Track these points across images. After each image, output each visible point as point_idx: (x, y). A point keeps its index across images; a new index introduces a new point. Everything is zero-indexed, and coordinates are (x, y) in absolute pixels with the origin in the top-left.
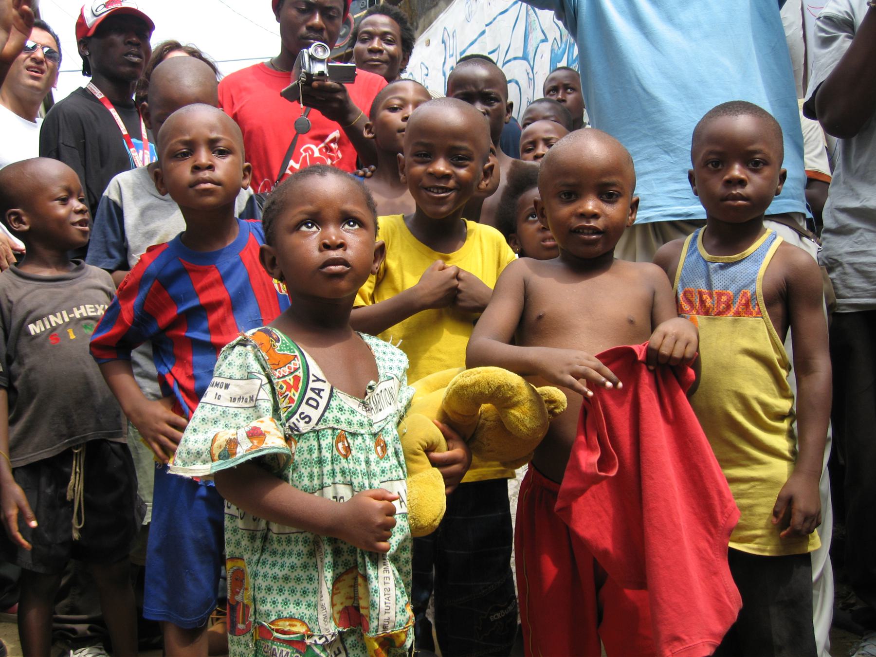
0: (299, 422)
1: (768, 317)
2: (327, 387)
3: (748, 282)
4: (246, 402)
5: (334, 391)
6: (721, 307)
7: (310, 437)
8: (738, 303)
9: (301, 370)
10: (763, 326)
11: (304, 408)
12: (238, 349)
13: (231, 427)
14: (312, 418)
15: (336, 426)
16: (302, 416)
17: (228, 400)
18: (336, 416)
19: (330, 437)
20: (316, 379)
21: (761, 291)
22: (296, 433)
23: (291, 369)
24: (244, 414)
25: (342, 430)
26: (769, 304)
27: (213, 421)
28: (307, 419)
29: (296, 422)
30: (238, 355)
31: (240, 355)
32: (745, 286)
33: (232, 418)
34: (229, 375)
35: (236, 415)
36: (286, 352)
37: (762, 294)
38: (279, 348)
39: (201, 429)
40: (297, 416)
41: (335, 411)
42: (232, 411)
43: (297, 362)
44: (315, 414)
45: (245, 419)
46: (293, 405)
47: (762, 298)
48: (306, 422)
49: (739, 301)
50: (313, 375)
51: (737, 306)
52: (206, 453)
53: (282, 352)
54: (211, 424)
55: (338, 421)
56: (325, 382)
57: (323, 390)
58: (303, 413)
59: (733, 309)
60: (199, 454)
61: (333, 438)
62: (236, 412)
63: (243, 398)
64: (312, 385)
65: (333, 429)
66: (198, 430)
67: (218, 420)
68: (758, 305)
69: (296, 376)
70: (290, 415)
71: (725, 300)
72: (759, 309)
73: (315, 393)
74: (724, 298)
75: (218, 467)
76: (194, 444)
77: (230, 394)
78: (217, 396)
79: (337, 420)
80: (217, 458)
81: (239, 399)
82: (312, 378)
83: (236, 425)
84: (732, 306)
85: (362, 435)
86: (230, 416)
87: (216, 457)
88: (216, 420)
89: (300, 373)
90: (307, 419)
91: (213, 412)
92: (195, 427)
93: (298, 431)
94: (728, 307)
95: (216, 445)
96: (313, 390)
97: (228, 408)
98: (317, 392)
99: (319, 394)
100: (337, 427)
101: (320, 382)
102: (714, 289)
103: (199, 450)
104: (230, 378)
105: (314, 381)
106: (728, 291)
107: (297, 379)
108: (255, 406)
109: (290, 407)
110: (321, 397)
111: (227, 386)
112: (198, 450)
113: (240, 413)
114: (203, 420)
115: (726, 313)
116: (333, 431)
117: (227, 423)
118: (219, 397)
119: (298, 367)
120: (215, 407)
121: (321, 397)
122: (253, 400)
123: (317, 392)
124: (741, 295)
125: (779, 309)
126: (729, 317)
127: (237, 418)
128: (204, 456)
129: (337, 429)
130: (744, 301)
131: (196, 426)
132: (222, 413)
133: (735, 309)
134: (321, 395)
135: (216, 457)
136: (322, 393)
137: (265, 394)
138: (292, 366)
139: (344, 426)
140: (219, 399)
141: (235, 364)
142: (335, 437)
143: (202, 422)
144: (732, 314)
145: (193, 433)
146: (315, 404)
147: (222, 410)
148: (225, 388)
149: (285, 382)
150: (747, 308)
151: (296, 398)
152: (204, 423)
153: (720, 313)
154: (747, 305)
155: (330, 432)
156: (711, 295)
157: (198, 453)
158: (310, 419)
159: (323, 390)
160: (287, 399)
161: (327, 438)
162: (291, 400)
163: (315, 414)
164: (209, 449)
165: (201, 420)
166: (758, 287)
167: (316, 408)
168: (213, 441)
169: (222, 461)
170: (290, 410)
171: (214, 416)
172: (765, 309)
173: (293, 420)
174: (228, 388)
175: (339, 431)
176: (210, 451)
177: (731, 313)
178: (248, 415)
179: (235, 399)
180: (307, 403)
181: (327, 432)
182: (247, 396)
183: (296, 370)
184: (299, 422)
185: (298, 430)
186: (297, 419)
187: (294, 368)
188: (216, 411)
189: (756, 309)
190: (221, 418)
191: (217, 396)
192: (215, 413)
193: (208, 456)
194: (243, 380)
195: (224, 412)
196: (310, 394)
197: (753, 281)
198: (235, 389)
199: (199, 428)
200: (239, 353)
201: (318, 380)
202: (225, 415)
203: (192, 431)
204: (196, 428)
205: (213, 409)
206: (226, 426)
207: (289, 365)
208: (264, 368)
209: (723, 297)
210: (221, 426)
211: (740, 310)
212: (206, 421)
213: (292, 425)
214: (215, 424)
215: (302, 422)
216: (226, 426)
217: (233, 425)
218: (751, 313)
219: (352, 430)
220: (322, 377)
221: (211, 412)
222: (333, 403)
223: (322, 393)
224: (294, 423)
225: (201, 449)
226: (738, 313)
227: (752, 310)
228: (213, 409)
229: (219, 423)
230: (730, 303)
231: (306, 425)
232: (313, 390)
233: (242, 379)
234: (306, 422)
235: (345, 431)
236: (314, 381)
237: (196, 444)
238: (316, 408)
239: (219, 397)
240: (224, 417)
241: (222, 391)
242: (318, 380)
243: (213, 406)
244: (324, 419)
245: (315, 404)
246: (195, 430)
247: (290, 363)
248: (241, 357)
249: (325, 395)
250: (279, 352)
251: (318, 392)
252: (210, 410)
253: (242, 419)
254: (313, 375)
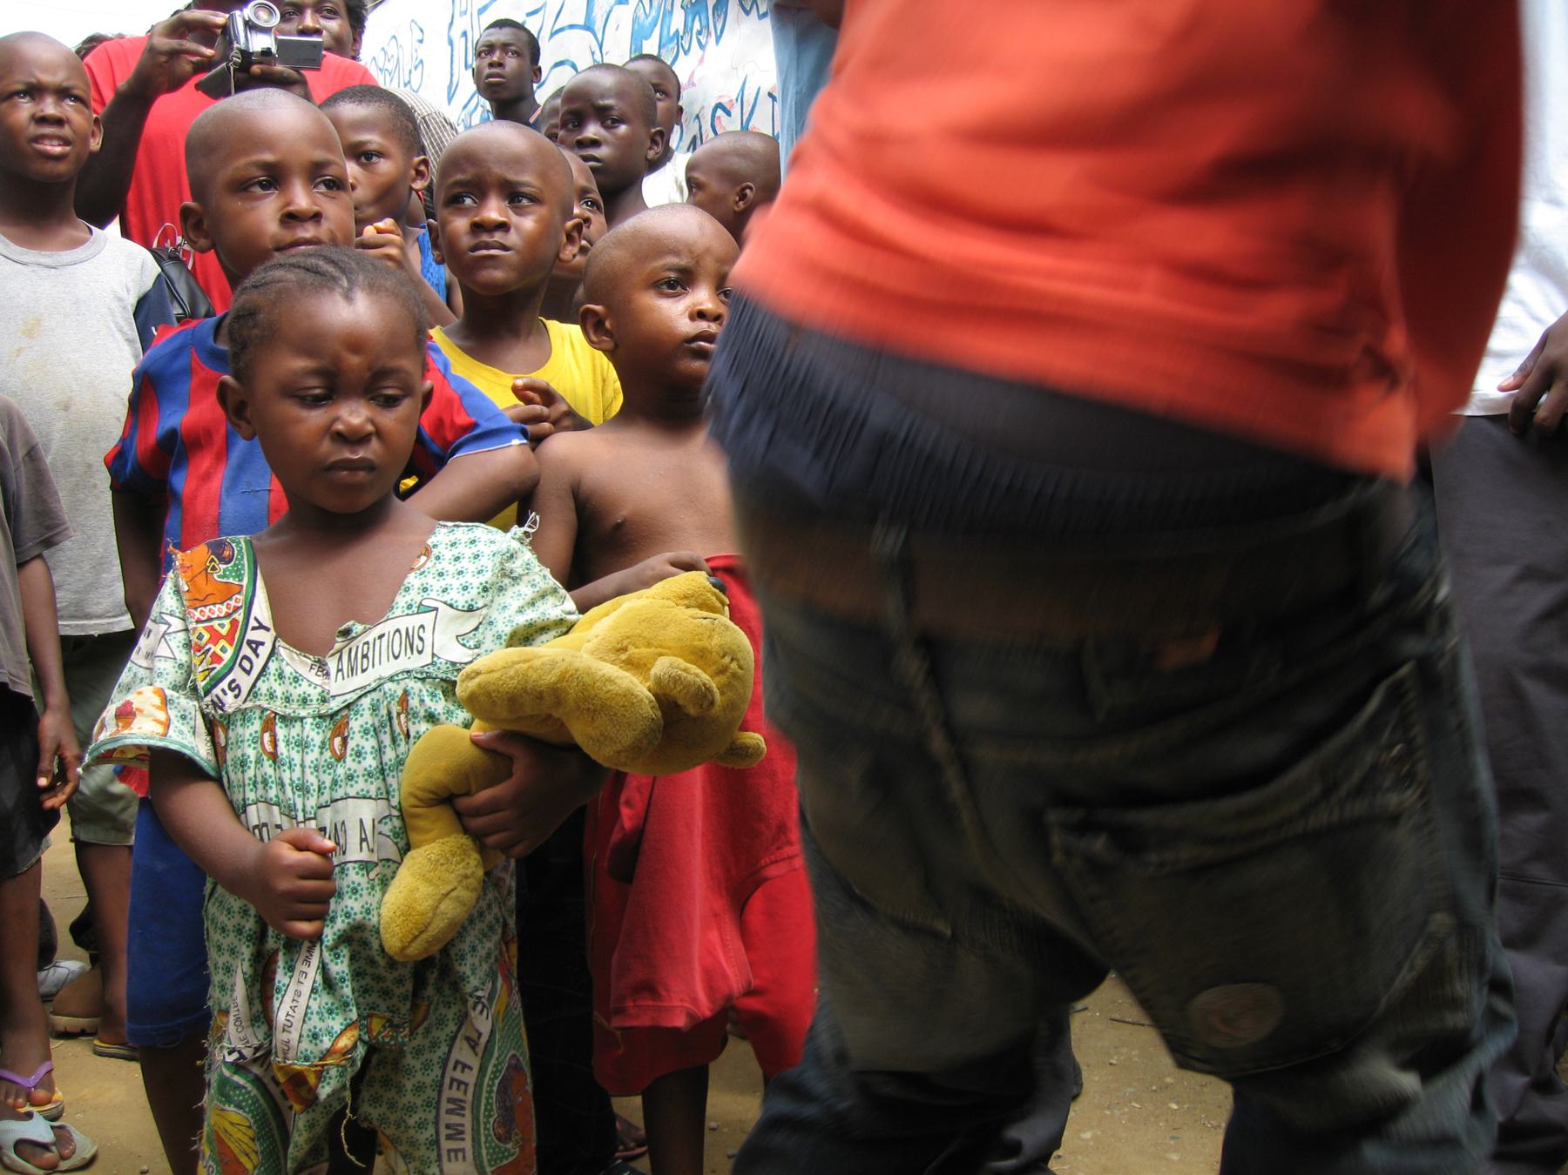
0: (225, 694)
5: (277, 644)
20: (257, 625)
22: (220, 712)
29: (221, 695)
36: (231, 580)
40: (224, 684)
44: (245, 682)
50: (256, 619)
53: (225, 580)
55: (272, 696)
57: (262, 644)
65: (264, 710)
70: (213, 683)
73: (251, 648)
79: (271, 694)
82: (253, 623)
85: (302, 719)
89: (240, 616)
93: (223, 710)
98: (254, 646)
99: (255, 651)
101: (262, 631)
105: (254, 629)
107: (234, 623)
109: (214, 668)
110: (257, 656)
119: (240, 605)
121: (257, 656)
123: (254, 646)
134: (259, 651)
138: (233, 603)
146: (246, 664)
149: (210, 629)
155: (258, 713)
159: (262, 644)
162: (217, 658)
163: (245, 682)
167: (248, 672)
170: (212, 674)
173: (217, 691)
175: (268, 712)
183: (236, 609)
184: (225, 694)
186: (223, 690)
187: (235, 607)
201: (261, 627)
213: (216, 700)
222: (273, 666)
223: (261, 650)
224: (217, 696)
232: (250, 643)
236: (254, 629)
242: (261, 627)
244: (256, 693)
245: (246, 664)
247: (230, 598)
249: (264, 651)
250: (219, 580)
251: (255, 645)
254: (256, 619)
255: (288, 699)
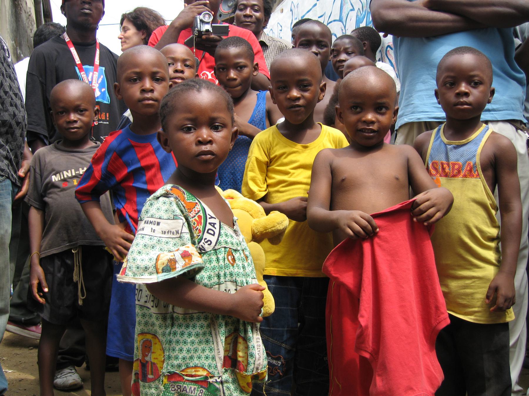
1: (484, 178)
2: (217, 221)
3: (471, 157)
4: (173, 234)
5: (222, 224)
6: (455, 172)
7: (211, 253)
8: (465, 170)
9: (201, 212)
10: (481, 183)
11: (206, 235)
12: (162, 199)
13: (164, 250)
14: (212, 241)
15: (226, 246)
16: (206, 241)
17: (160, 232)
18: (225, 240)
19: (223, 253)
20: (210, 217)
21: (479, 162)
22: (203, 251)
23: (196, 212)
24: (172, 242)
25: (230, 248)
26: (484, 170)
27: (152, 247)
28: (209, 243)
29: (203, 245)
30: (163, 203)
31: (164, 203)
32: (469, 159)
33: (165, 244)
34: (159, 216)
35: (167, 243)
37: (479, 164)
38: (186, 199)
39: (144, 252)
40: (203, 241)
41: (224, 236)
42: (164, 240)
43: (198, 207)
44: (214, 239)
45: (173, 245)
46: (201, 234)
47: (480, 166)
48: (209, 245)
49: (466, 168)
51: (464, 172)
52: (153, 268)
53: (189, 201)
54: (150, 248)
55: (226, 243)
56: (215, 218)
58: (206, 239)
59: (462, 173)
60: (146, 268)
61: (225, 254)
62: (167, 241)
63: (171, 232)
64: (209, 221)
65: (225, 248)
66: (142, 252)
67: (154, 246)
68: (477, 171)
69: (199, 215)
71: (457, 167)
72: (478, 173)
73: (212, 225)
74: (456, 167)
75: (164, 277)
76: (142, 262)
77: (162, 229)
78: (153, 230)
79: (226, 242)
80: (161, 271)
81: (168, 232)
83: (168, 249)
84: (461, 171)
86: (163, 243)
87: (160, 270)
88: (153, 246)
89: (201, 214)
90: (209, 243)
91: (151, 241)
92: (139, 250)
94: (459, 172)
95: (160, 262)
96: (210, 224)
97: (161, 238)
98: (213, 225)
99: (214, 226)
100: (227, 247)
101: (213, 219)
102: (450, 161)
103: (147, 266)
104: (160, 218)
105: (210, 218)
106: (459, 162)
107: (200, 217)
108: (180, 237)
109: (200, 235)
111: (158, 224)
112: (145, 266)
113: (170, 241)
114: (145, 246)
115: (458, 175)
116: (225, 249)
117: (161, 248)
118: (154, 231)
119: (199, 210)
120: (152, 237)
121: (215, 228)
122: (178, 233)
124: (467, 165)
125: (490, 173)
126: (460, 178)
127: (168, 245)
128: (150, 270)
129: (227, 248)
130: (468, 168)
131: (140, 250)
132: (157, 241)
133: (463, 173)
134: (215, 227)
135: (160, 270)
136: (215, 225)
137: (186, 229)
138: (196, 209)
139: (230, 246)
140: (154, 232)
141: (162, 209)
142: (226, 252)
143: (144, 247)
144: (462, 176)
145: (139, 254)
146: (212, 233)
147: (158, 240)
148: (157, 225)
149: (195, 220)
150: (471, 173)
151: (201, 229)
152: (146, 248)
153: (454, 176)
154: (470, 171)
156: (448, 165)
157: (146, 268)
158: (211, 242)
159: (216, 224)
160: (197, 231)
161: (222, 253)
162: (200, 230)
163: (214, 239)
164: (154, 265)
165: (143, 246)
166: (477, 160)
167: (214, 235)
168: (157, 260)
169: (165, 274)
170: (199, 237)
171: (152, 243)
172: (482, 173)
173: (201, 243)
174: (159, 225)
176: (155, 266)
177: (461, 176)
178: (175, 243)
179: (165, 232)
180: (208, 232)
181: (221, 250)
182: (174, 230)
183: (199, 211)
184: (205, 244)
185: (204, 250)
186: (203, 243)
187: (198, 211)
188: (153, 240)
189: (476, 173)
190: (157, 244)
191: (153, 230)
192: (153, 241)
193: (154, 269)
194: (170, 219)
195: (159, 241)
196: (208, 227)
197: (474, 156)
198: (165, 225)
199: (142, 251)
200: (163, 202)
201: (212, 217)
202: (159, 243)
203: (138, 253)
204: (141, 251)
205: (151, 239)
206: (161, 249)
207: (194, 209)
208: (182, 211)
209: (456, 166)
210: (157, 250)
211: (466, 174)
212: (147, 247)
213: (201, 247)
214: (153, 248)
215: (206, 244)
216: (161, 249)
217: (166, 249)
218: (473, 176)
219: (235, 248)
220: (213, 216)
221: (150, 240)
224: (202, 246)
225: (148, 265)
226: (465, 176)
227: (474, 174)
228: (151, 239)
229: (155, 247)
230: (460, 169)
231: (209, 246)
232: (210, 224)
233: (169, 219)
234: (209, 245)
235: (231, 249)
236: (210, 218)
237: (143, 262)
238: (214, 235)
239: (154, 231)
240: (158, 244)
241: (155, 227)
242: (212, 217)
243: (151, 237)
244: (219, 242)
245: (212, 233)
246: (140, 253)
247: (194, 207)
248: (165, 205)
249: (217, 226)
251: (213, 225)
252: (149, 239)
253: (171, 245)
255: (232, 244)
